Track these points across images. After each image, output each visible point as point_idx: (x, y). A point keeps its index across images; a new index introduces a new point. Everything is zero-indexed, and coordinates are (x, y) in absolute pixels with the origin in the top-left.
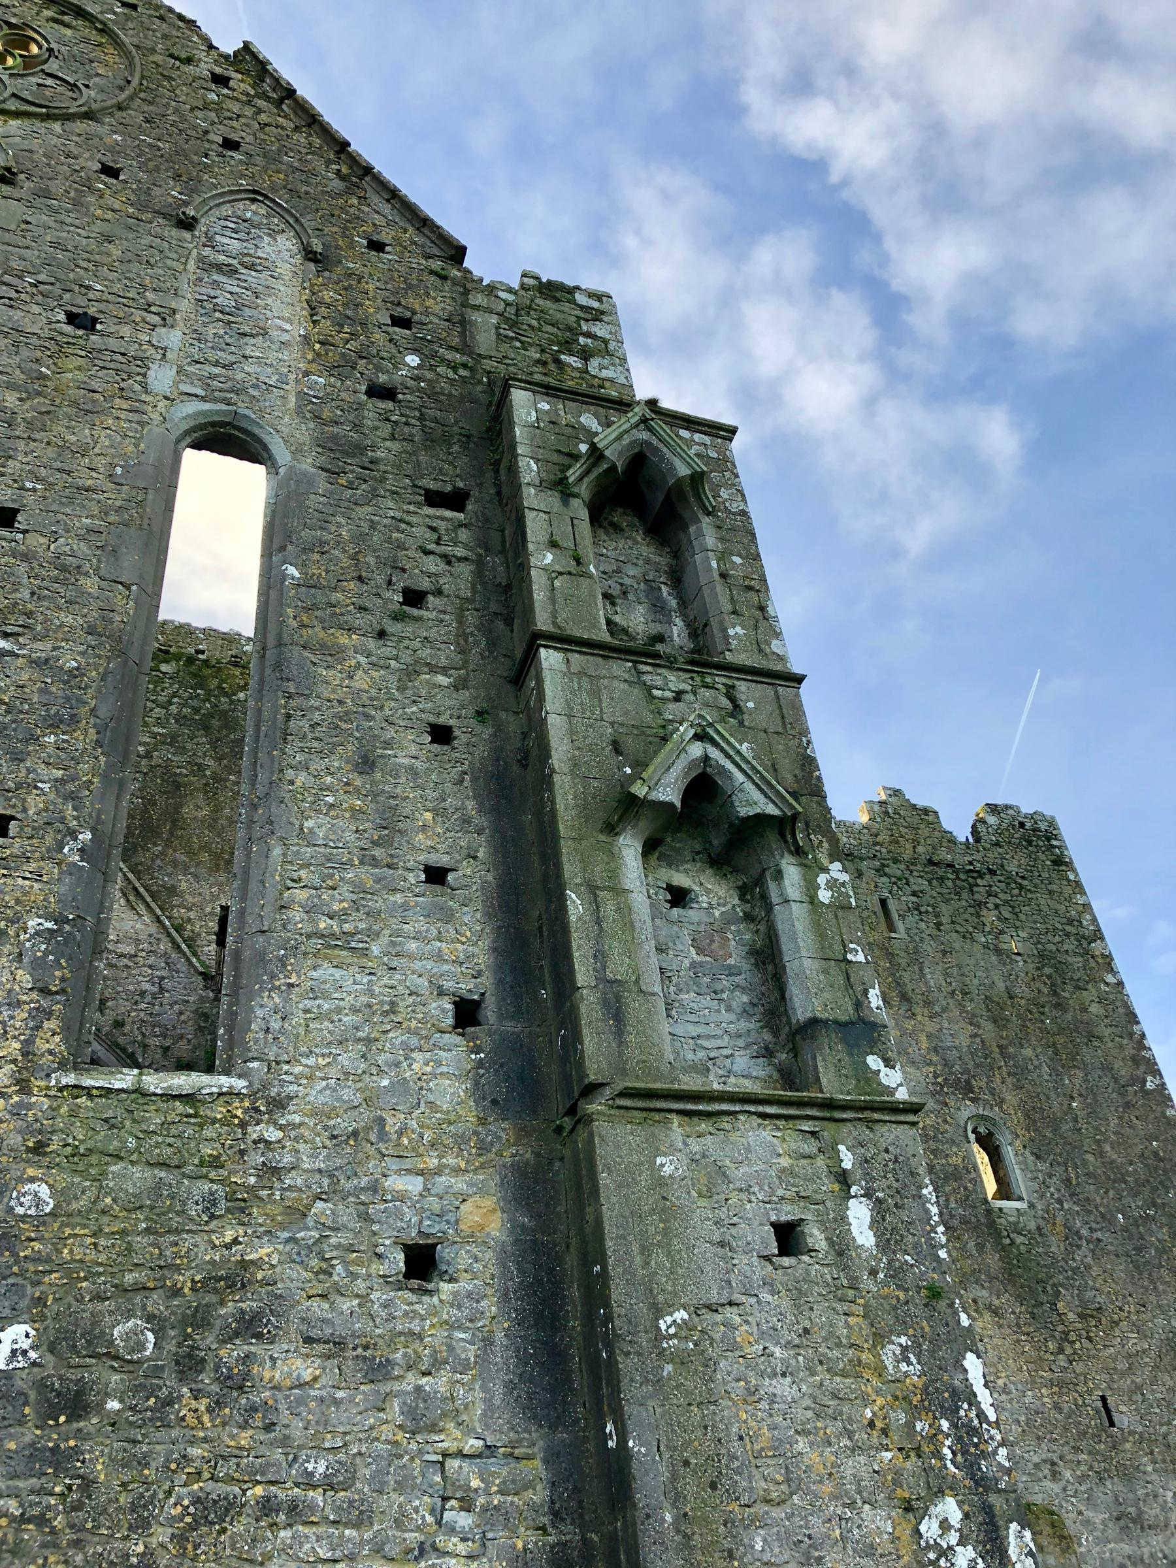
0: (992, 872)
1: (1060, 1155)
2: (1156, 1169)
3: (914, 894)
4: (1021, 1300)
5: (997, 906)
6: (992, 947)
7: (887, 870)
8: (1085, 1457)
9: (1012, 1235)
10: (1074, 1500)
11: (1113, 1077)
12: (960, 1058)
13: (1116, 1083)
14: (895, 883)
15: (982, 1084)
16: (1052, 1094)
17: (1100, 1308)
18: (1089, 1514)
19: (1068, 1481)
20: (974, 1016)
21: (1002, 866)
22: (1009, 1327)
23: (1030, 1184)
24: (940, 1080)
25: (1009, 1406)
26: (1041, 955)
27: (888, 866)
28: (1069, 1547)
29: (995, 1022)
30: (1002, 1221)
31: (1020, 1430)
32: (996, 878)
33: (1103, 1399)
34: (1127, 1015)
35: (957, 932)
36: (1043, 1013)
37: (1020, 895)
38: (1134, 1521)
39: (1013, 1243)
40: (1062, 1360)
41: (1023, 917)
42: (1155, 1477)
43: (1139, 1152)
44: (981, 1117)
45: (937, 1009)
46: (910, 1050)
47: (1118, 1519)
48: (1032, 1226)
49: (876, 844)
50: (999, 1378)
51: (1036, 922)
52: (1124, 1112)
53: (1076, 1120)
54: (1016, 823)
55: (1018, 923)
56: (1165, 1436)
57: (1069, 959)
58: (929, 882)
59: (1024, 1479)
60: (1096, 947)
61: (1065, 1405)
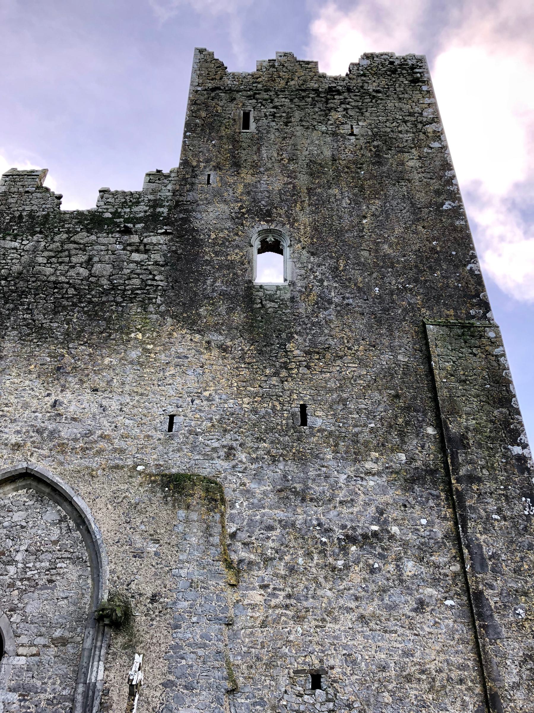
0: (349, 90)
1: (335, 253)
2: (427, 258)
3: (275, 107)
4: (252, 342)
5: (346, 109)
6: (329, 132)
7: (257, 96)
8: (266, 445)
9: (264, 302)
10: (240, 475)
11: (411, 203)
12: (268, 197)
13: (413, 206)
14: (261, 103)
15: (282, 212)
16: (346, 216)
17: (328, 348)
18: (252, 486)
19: (241, 462)
20: (295, 172)
21: (362, 87)
22: (233, 358)
23: (297, 270)
24: (244, 210)
25: (207, 409)
26: (375, 135)
27: (259, 94)
28: (216, 507)
29: (311, 175)
30: (261, 294)
31: (210, 425)
32: (351, 94)
33: (303, 408)
34: (442, 165)
35: (303, 126)
36: (360, 168)
37: (371, 102)
38: (296, 493)
39: (263, 306)
40: (274, 381)
41: (367, 114)
42: (333, 463)
43: (415, 248)
45: (262, 169)
46: (225, 194)
47: (280, 491)
49: (256, 82)
50: (206, 390)
51: (378, 117)
52: (413, 224)
53: (362, 231)
54: (387, 63)
55: (360, 118)
56: (356, 435)
57: (401, 136)
58: (291, 100)
59: (197, 457)
60: (430, 128)
61: (263, 409)
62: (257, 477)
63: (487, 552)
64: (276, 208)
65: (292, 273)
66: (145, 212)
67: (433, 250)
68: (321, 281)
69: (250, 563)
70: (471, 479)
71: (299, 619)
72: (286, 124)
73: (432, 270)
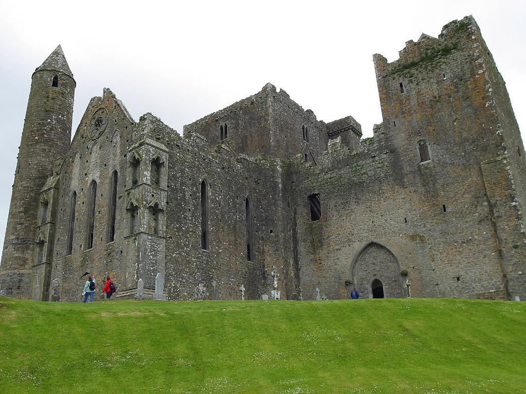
44: (421, 140)
48: (432, 166)
62: (434, 230)
63: (503, 238)
64: (421, 129)
65: (432, 155)
66: (377, 146)
67: (482, 129)
68: (443, 156)
69: (437, 254)
70: (499, 217)
71: (451, 266)
72: (417, 84)
73: (483, 138)
